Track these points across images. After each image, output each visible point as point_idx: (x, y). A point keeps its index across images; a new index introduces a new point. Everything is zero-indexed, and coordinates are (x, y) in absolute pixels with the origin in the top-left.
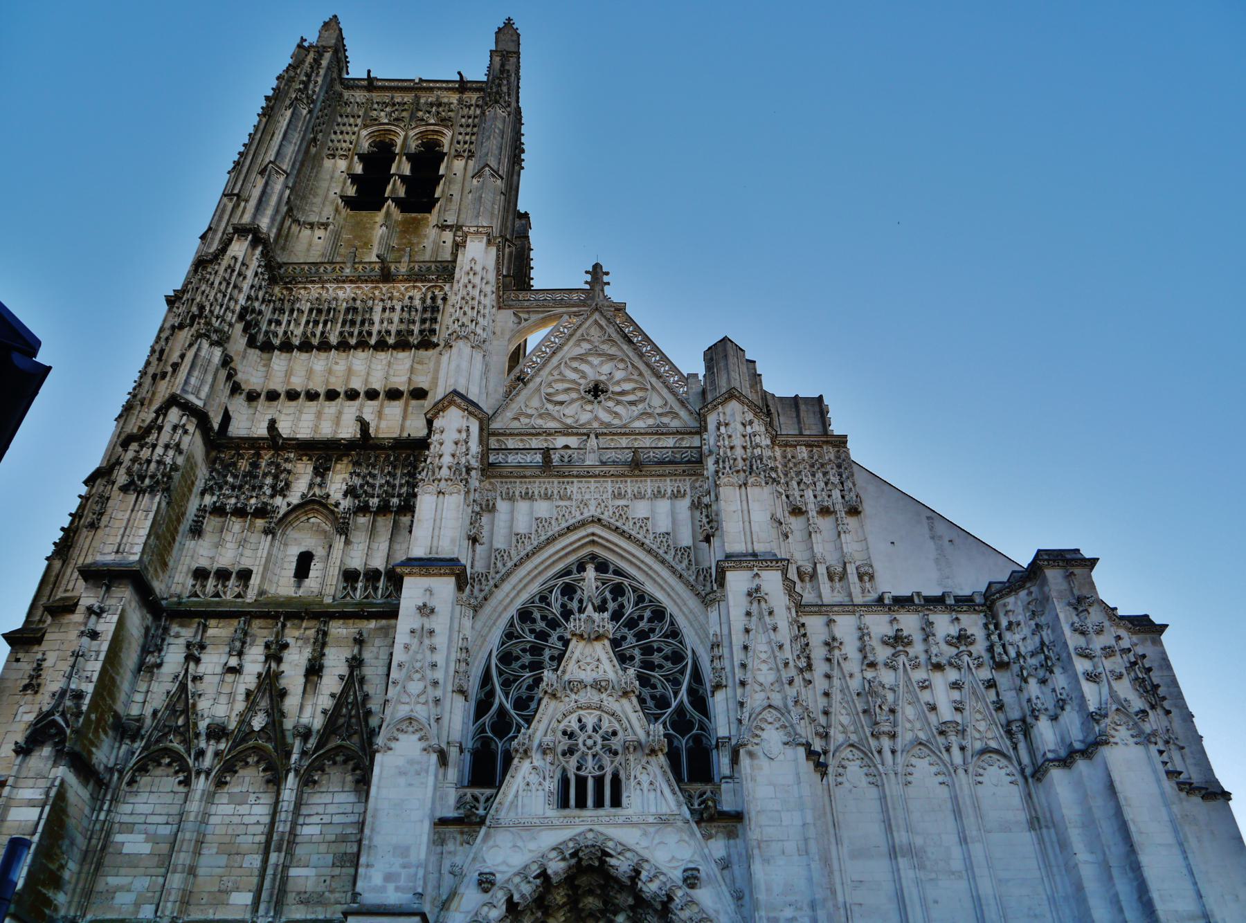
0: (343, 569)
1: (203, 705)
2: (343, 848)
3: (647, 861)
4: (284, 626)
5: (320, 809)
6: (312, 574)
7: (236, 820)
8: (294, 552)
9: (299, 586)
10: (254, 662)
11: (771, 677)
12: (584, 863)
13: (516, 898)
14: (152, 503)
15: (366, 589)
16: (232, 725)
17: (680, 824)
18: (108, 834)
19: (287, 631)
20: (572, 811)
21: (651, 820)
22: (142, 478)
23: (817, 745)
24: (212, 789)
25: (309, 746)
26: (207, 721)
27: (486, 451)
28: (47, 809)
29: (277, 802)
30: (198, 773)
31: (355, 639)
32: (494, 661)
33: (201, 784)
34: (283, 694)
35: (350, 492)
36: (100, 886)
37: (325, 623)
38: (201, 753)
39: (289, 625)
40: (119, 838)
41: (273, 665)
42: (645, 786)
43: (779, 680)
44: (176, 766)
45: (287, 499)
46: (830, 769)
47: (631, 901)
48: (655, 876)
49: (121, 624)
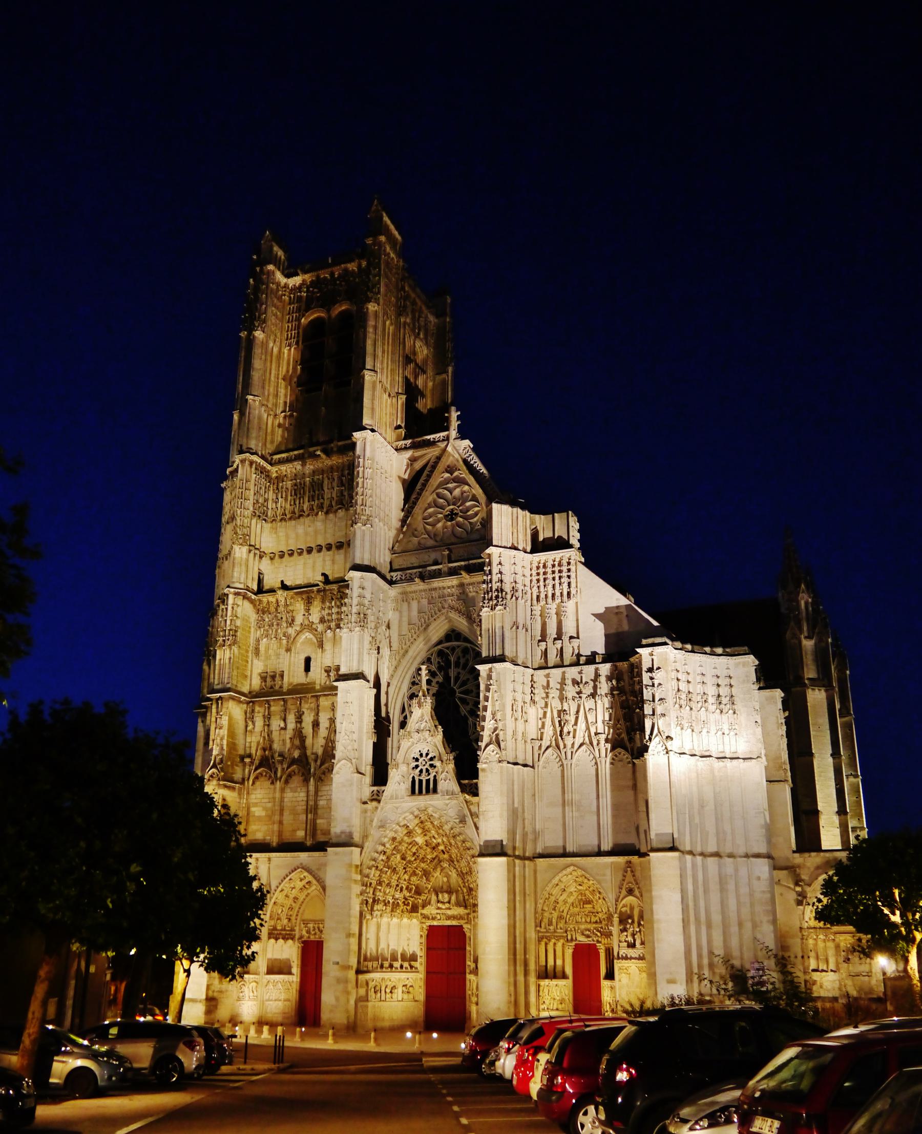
4: (300, 704)
5: (325, 793)
6: (312, 669)
7: (294, 799)
8: (302, 658)
9: (307, 677)
10: (291, 723)
18: (248, 809)
19: (302, 705)
29: (308, 792)
32: (406, 699)
35: (322, 620)
37: (317, 700)
39: (303, 701)
41: (298, 725)
45: (294, 628)
49: (230, 719)
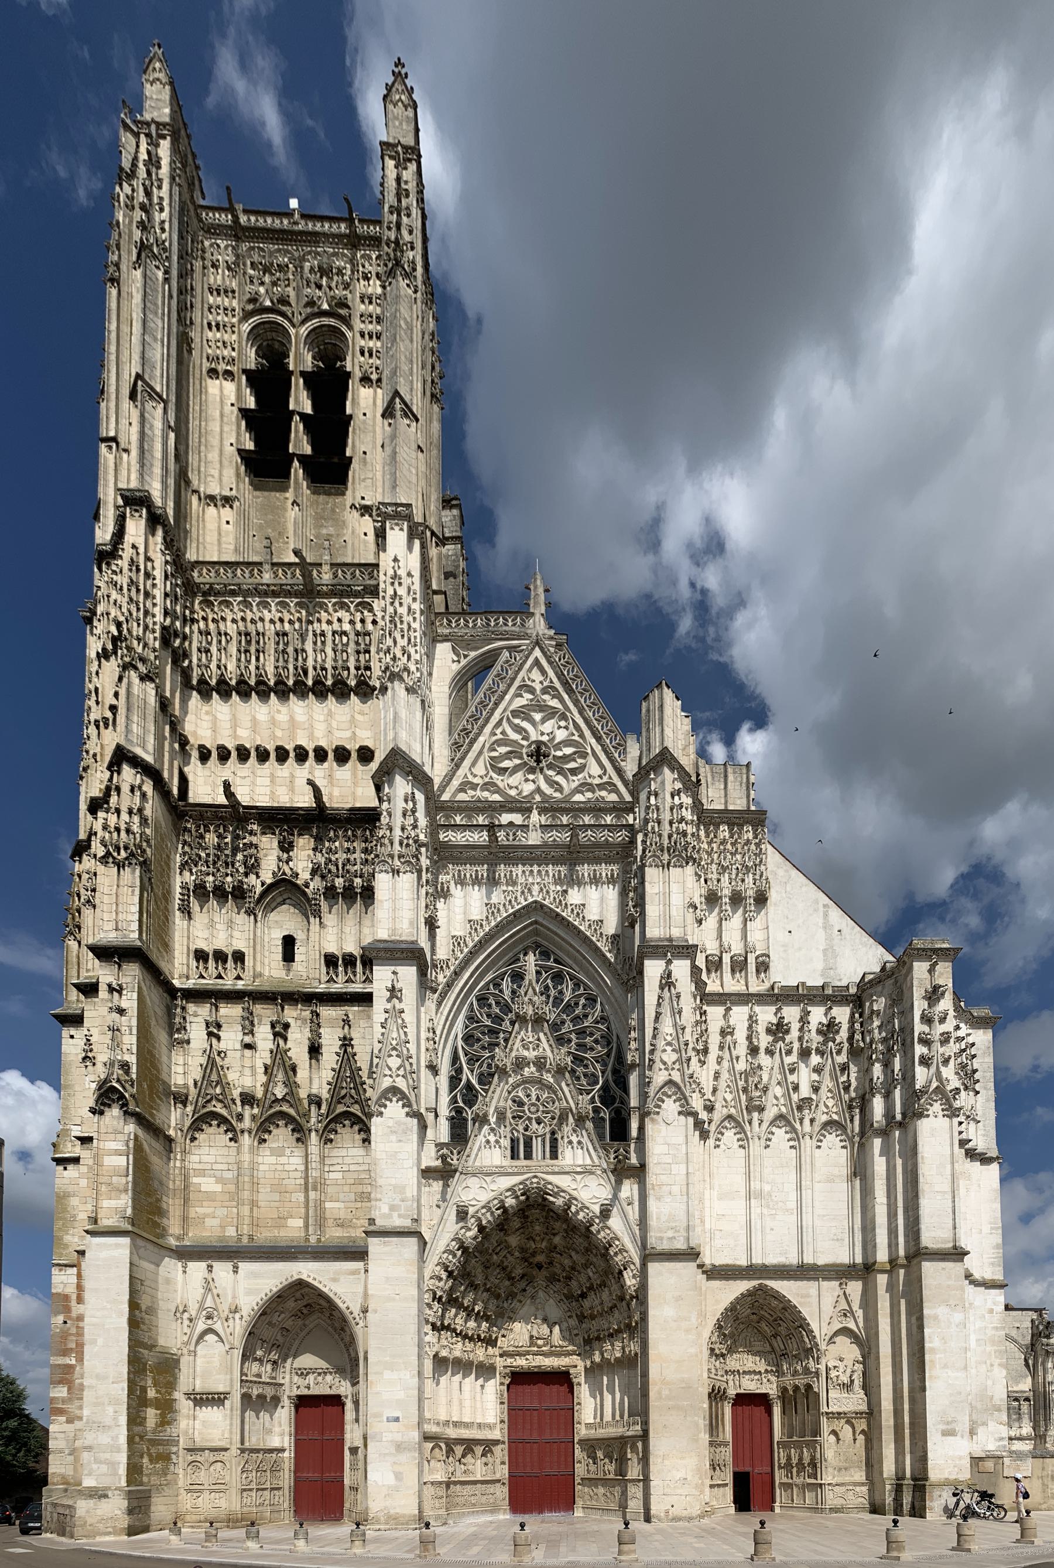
0: (323, 953)
1: (232, 1076)
2: (360, 1189)
3: (576, 1199)
10: (265, 1039)
11: (674, 1056)
12: (531, 1200)
13: (484, 1222)
14: (134, 878)
15: (346, 973)
16: (259, 1093)
17: (599, 1172)
18: (186, 1178)
20: (522, 1162)
21: (579, 1169)
22: (118, 849)
23: (703, 1115)
24: (256, 1143)
25: (322, 1111)
26: (239, 1090)
27: (434, 828)
28: (131, 1157)
30: (242, 1132)
31: (344, 1020)
33: (246, 1140)
34: (294, 1069)
36: (192, 1214)
38: (240, 1117)
40: (195, 1180)
42: (575, 1145)
43: (679, 1060)
44: (223, 1128)
46: (711, 1134)
47: (564, 1226)
48: (581, 1209)
